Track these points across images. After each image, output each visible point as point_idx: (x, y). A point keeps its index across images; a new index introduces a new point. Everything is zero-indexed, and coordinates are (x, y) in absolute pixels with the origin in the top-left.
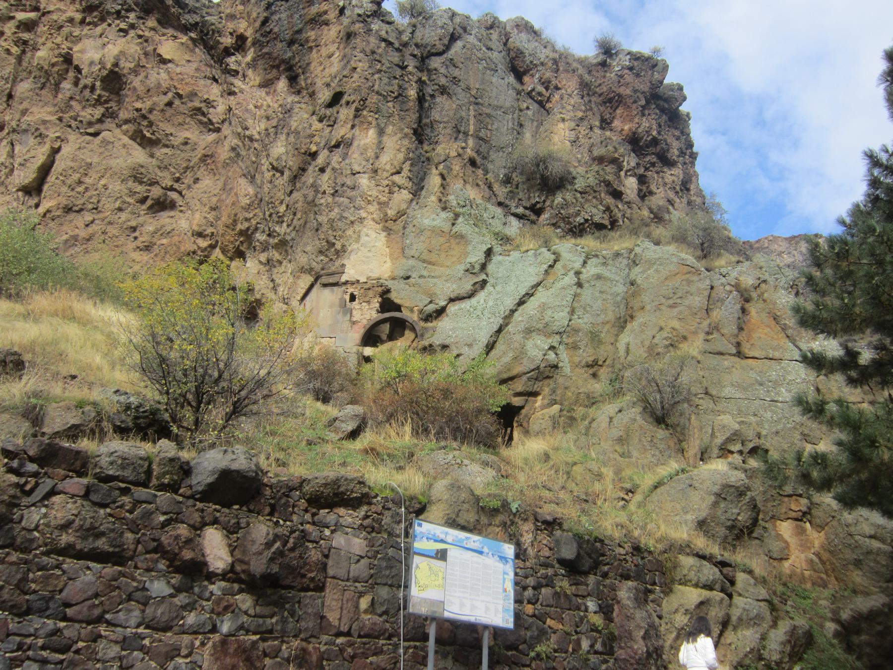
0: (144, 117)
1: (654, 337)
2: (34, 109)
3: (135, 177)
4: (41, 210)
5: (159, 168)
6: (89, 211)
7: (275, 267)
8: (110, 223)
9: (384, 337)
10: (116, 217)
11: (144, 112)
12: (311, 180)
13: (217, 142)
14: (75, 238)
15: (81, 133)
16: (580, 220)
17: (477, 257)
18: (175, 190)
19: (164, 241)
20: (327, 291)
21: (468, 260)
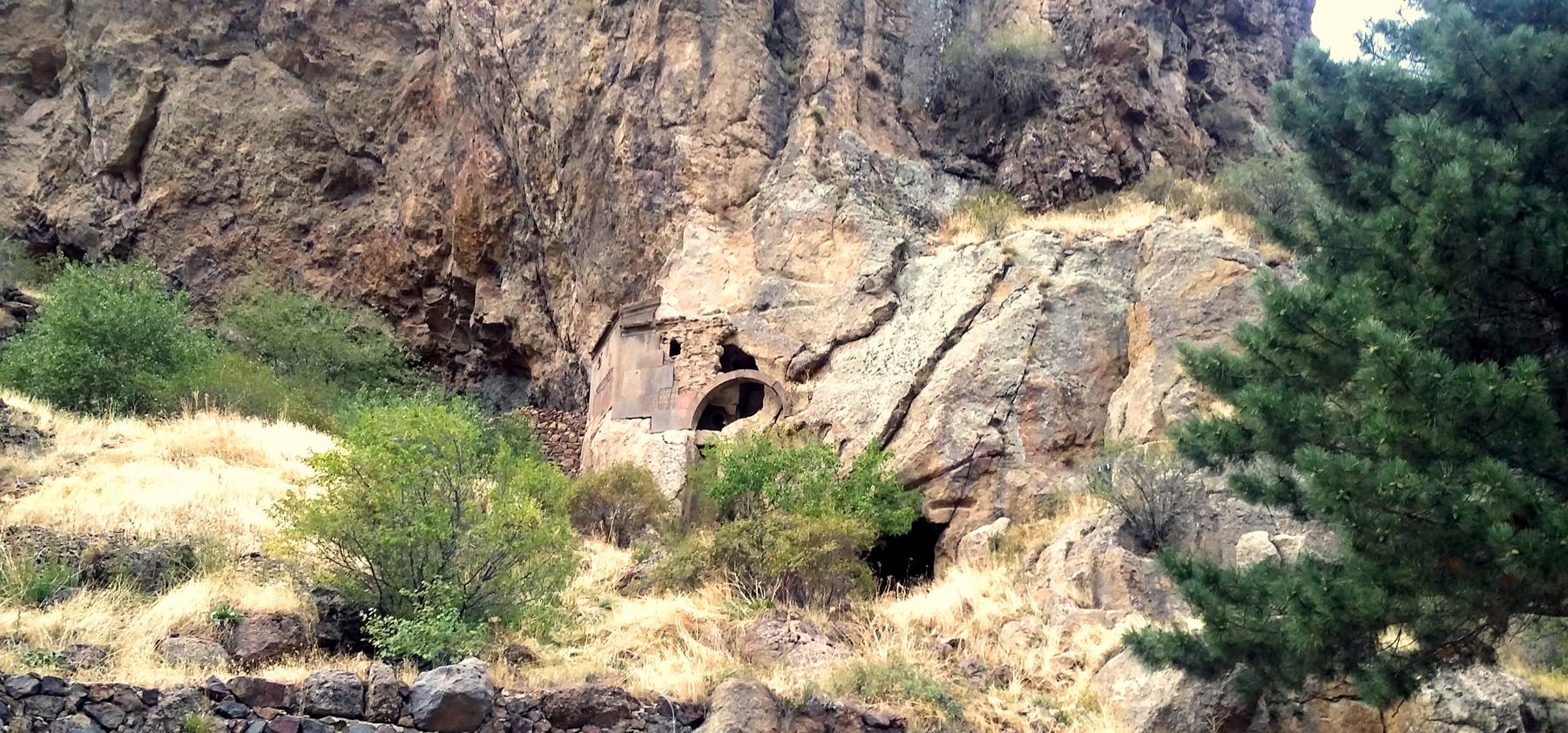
0: (301, 28)
1: (1165, 394)
2: (113, 26)
3: (298, 137)
4: (143, 206)
5: (338, 117)
6: (224, 202)
7: (550, 287)
8: (263, 221)
9: (732, 409)
10: (273, 210)
11: (300, 18)
12: (597, 139)
13: (433, 67)
14: (206, 251)
15: (196, 62)
16: (1064, 174)
17: (880, 262)
18: (369, 155)
19: (359, 248)
20: (632, 341)
21: (865, 270)
